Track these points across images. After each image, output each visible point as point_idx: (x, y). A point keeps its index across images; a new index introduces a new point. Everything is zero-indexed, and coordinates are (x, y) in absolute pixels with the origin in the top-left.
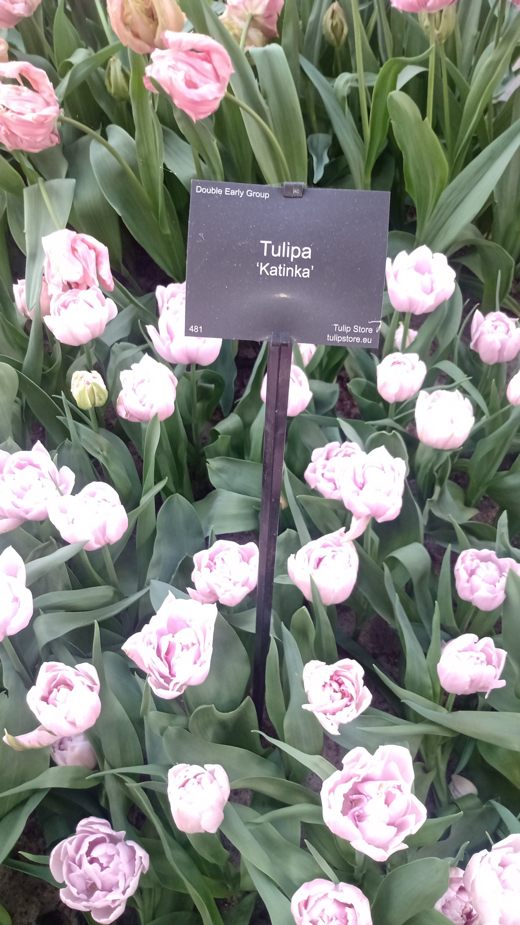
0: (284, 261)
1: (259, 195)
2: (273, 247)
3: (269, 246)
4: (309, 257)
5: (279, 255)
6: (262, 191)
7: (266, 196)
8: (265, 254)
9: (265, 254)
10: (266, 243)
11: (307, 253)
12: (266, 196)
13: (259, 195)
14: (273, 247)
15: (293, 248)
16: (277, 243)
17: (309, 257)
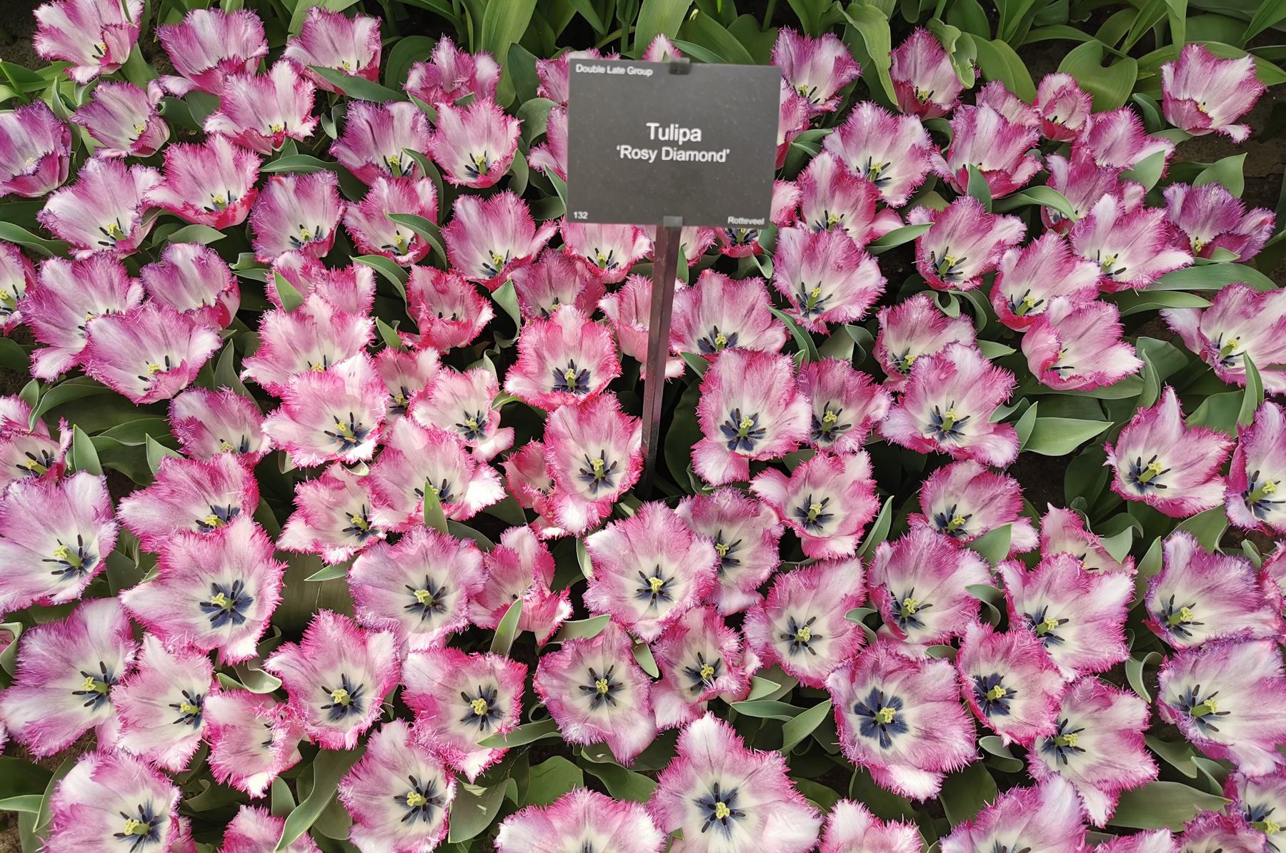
0: (673, 144)
1: (641, 72)
2: (660, 130)
3: (657, 129)
4: (699, 139)
5: (666, 138)
6: (645, 68)
7: (649, 73)
8: (652, 137)
9: (652, 137)
10: (653, 125)
11: (696, 135)
12: (649, 73)
13: (641, 72)
14: (660, 130)
15: (682, 131)
16: (665, 125)
17: (699, 139)
